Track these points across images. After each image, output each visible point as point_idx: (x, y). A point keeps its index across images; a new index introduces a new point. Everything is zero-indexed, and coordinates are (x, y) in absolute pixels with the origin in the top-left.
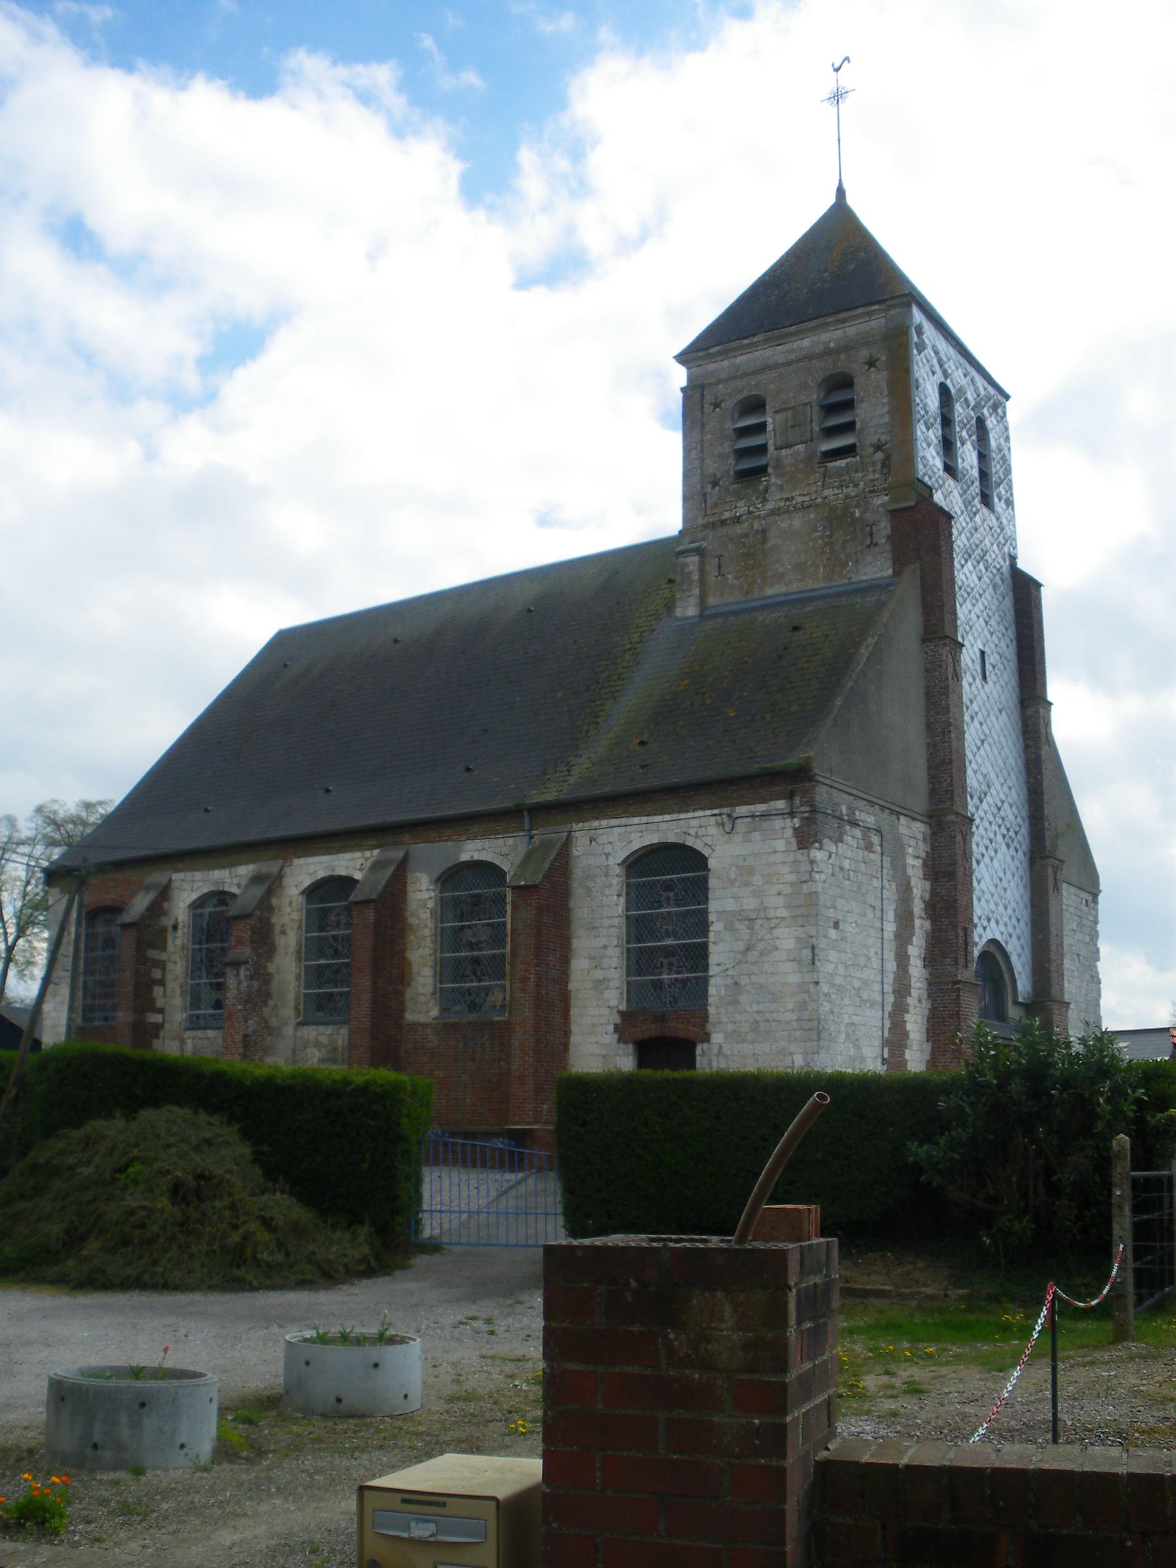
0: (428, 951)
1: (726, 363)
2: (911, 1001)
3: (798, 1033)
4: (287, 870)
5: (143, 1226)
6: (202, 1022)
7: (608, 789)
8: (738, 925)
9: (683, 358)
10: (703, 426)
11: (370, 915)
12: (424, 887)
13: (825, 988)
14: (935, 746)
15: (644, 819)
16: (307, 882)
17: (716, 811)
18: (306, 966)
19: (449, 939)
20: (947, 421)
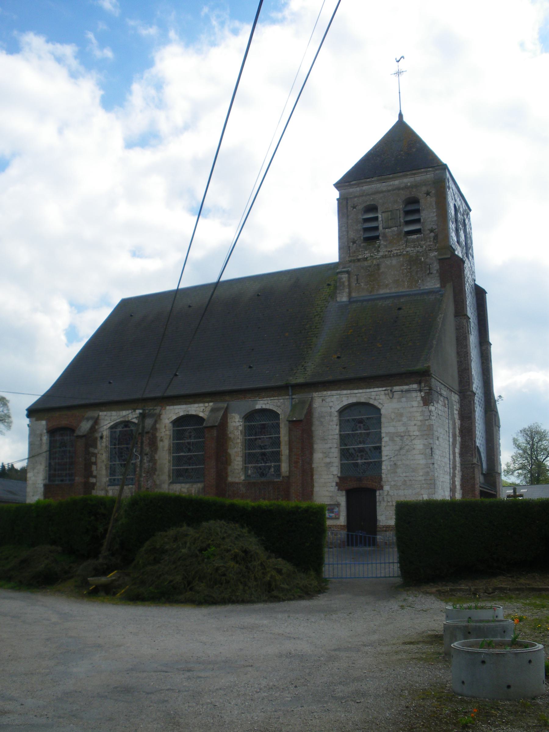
0: (239, 450)
1: (358, 189)
2: (457, 472)
3: (425, 485)
4: (163, 412)
5: (224, 575)
6: (116, 482)
7: (330, 378)
8: (396, 439)
9: (338, 185)
10: (348, 216)
11: (215, 433)
12: (237, 420)
13: (436, 466)
14: (461, 362)
15: (349, 392)
16: (174, 417)
17: (384, 389)
18: (173, 456)
19: (249, 444)
20: (456, 221)
